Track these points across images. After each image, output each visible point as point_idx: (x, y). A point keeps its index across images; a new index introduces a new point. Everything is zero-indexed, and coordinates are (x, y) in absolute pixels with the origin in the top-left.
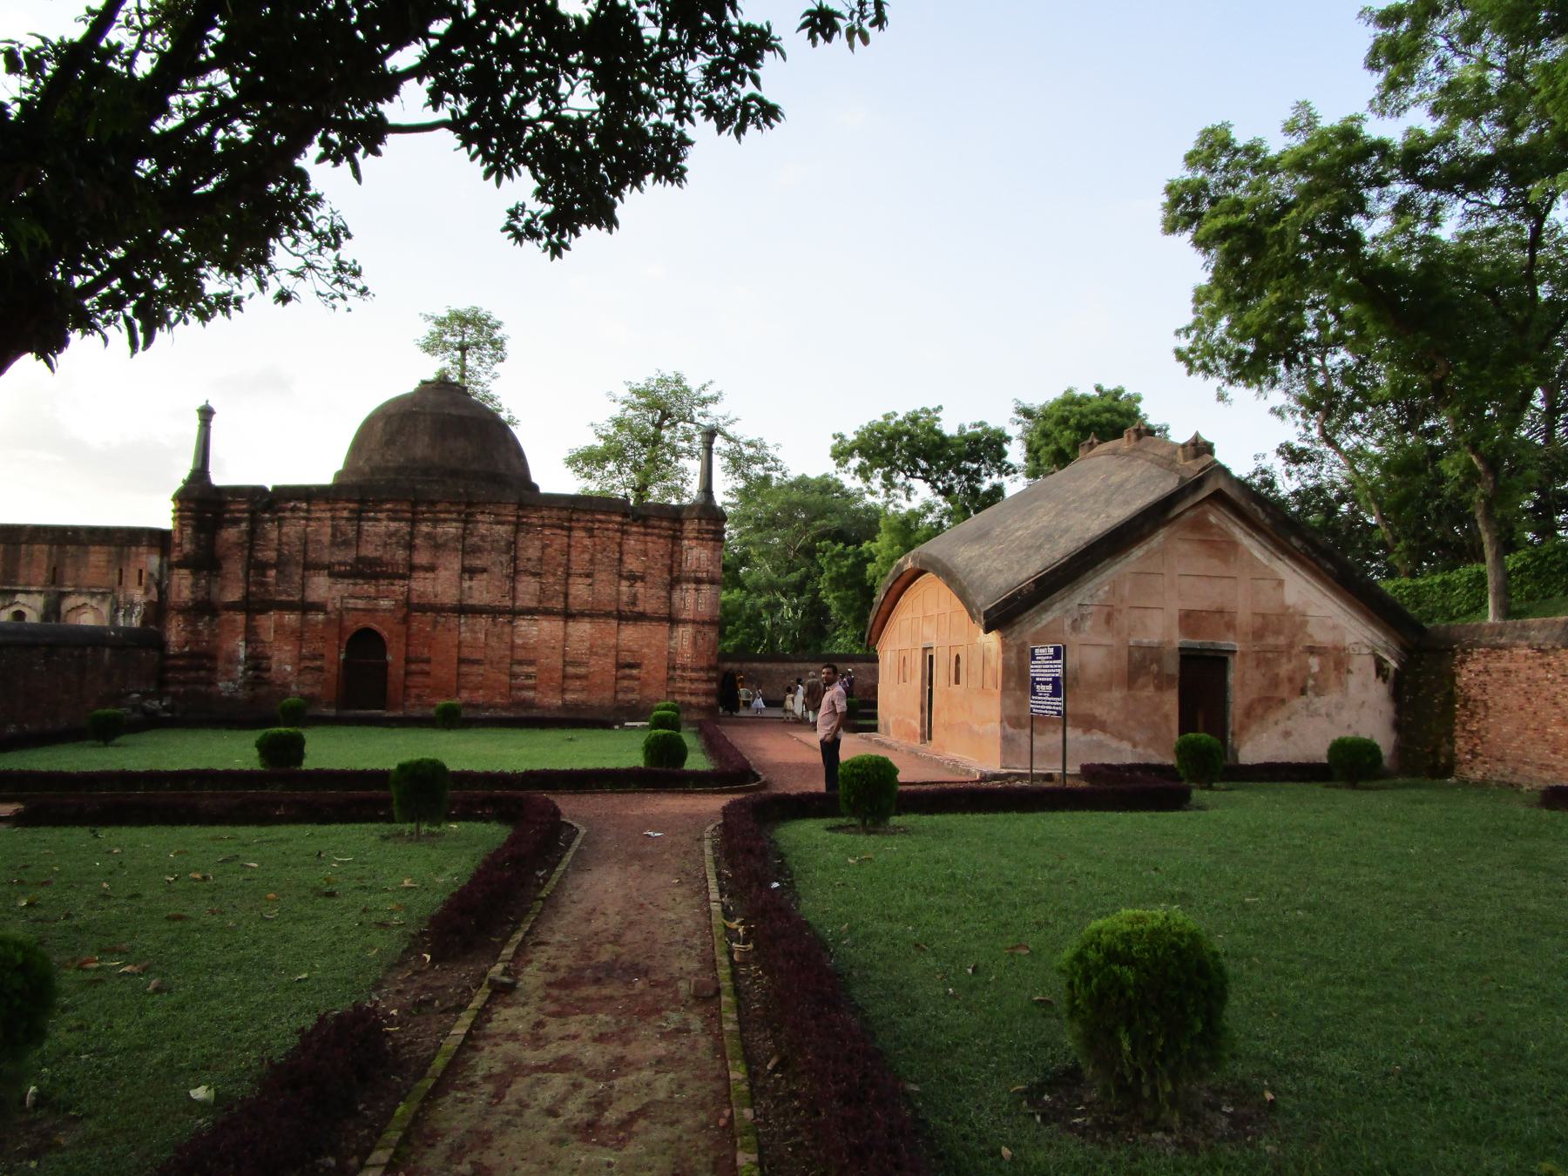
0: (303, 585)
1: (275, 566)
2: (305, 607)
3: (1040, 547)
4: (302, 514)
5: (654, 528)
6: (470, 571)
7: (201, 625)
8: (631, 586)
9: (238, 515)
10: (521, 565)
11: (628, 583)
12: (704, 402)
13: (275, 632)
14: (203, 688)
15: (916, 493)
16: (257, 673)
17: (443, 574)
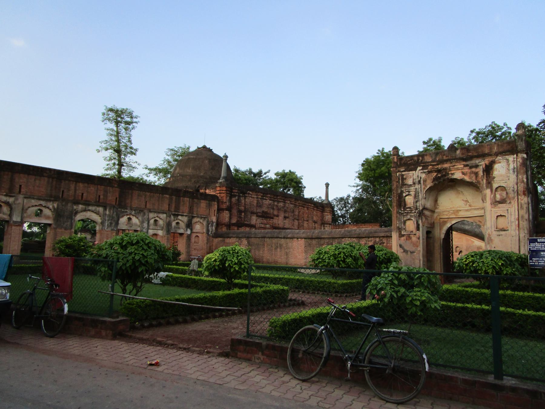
4: (250, 196)
6: (285, 218)
9: (235, 194)
17: (280, 218)
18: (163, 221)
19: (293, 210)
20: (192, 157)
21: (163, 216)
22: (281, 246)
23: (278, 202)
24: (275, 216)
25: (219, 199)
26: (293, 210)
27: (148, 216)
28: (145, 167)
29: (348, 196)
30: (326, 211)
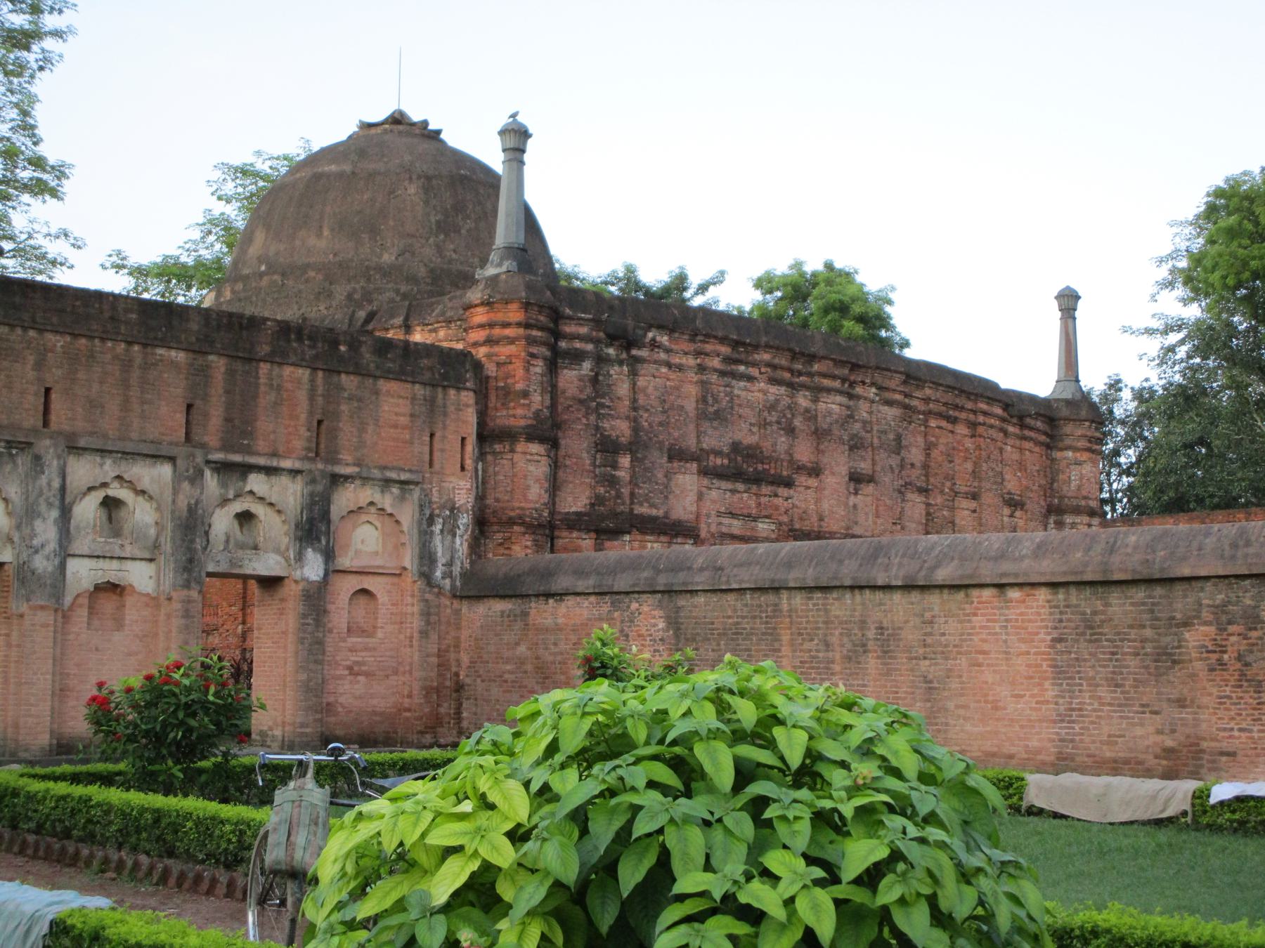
4: (663, 356)
5: (1031, 429)
6: (856, 479)
9: (578, 345)
18: (158, 509)
19: (898, 438)
20: (333, 168)
21: (157, 475)
22: (887, 639)
23: (817, 392)
24: (800, 468)
25: (488, 377)
26: (898, 438)
27: (63, 476)
28: (114, 258)
29: (1111, 386)
30: (1068, 442)
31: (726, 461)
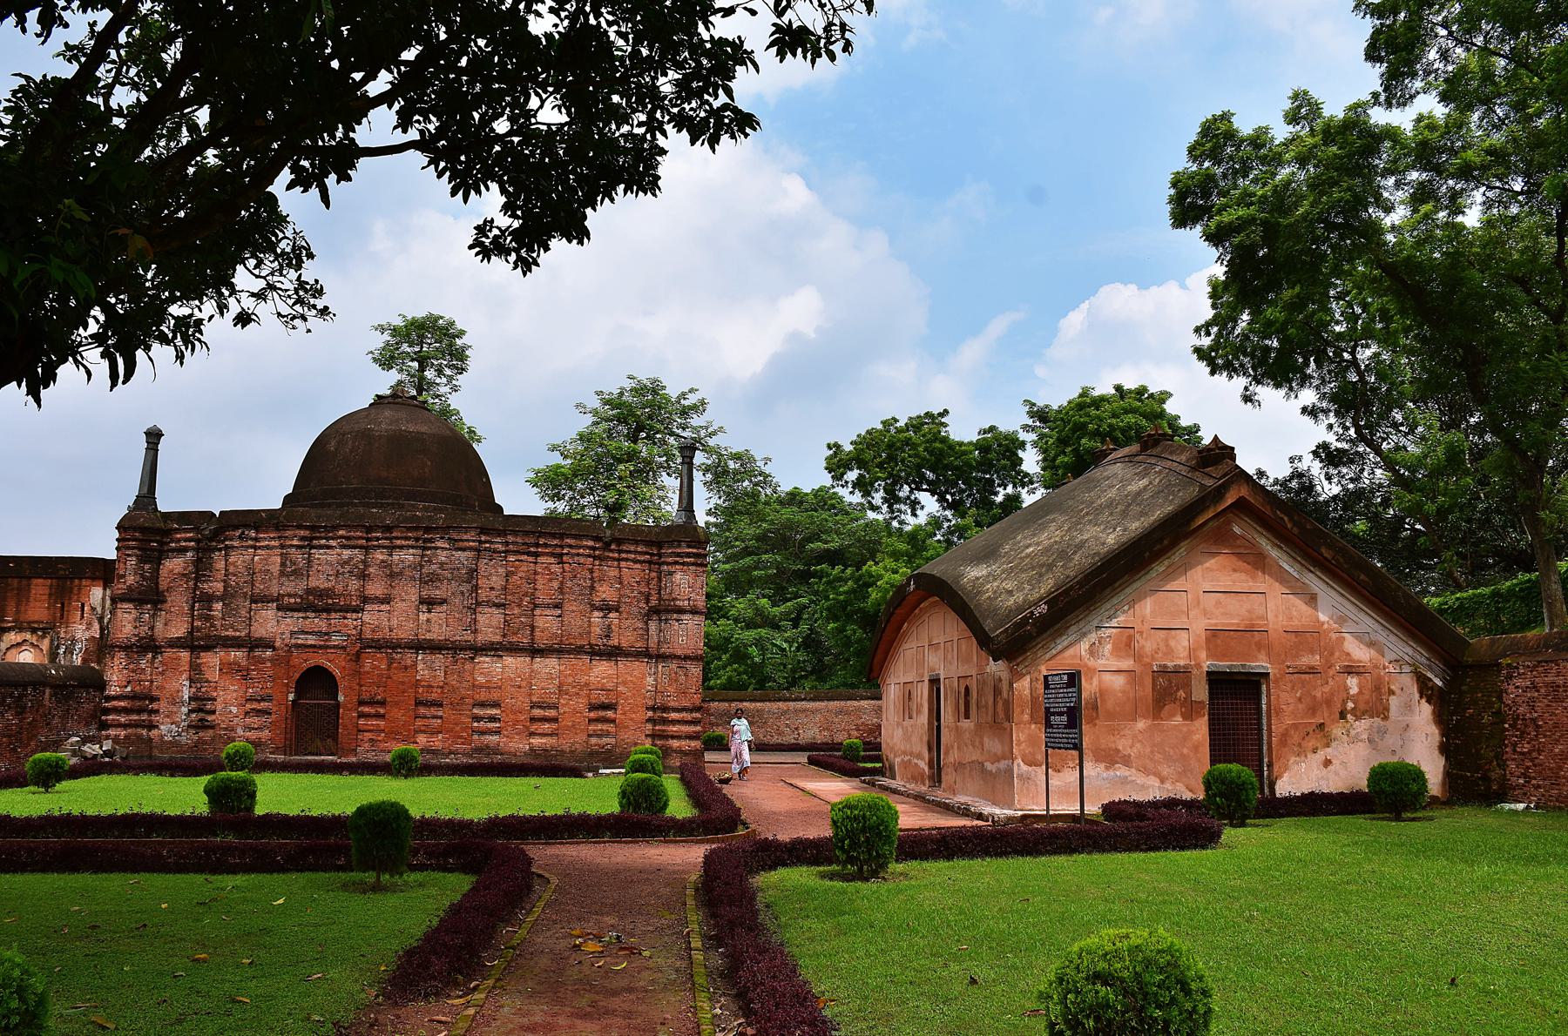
0: (250, 619)
1: (221, 598)
2: (252, 644)
3: (1050, 567)
4: (250, 542)
6: (429, 603)
7: (143, 664)
8: (605, 617)
10: (483, 594)
11: (602, 614)
12: (685, 412)
13: (220, 670)
14: (144, 732)
15: (922, 508)
16: (201, 715)
31: (298, 600)
